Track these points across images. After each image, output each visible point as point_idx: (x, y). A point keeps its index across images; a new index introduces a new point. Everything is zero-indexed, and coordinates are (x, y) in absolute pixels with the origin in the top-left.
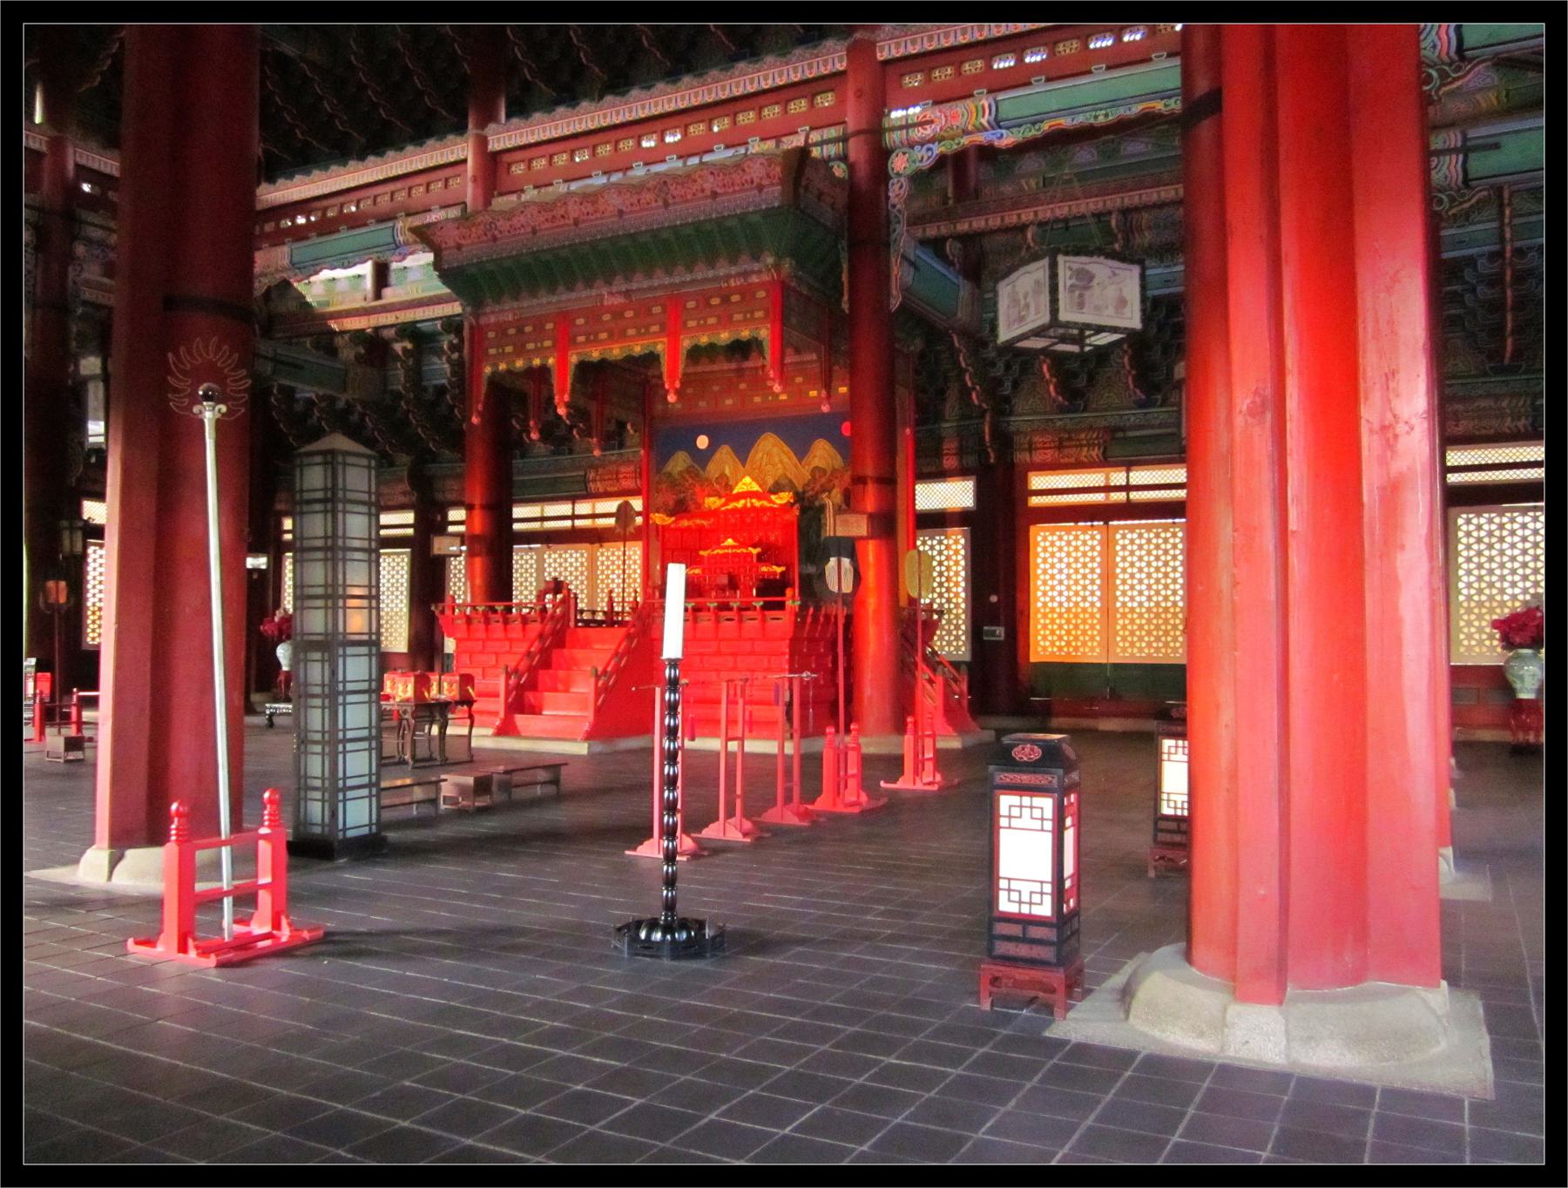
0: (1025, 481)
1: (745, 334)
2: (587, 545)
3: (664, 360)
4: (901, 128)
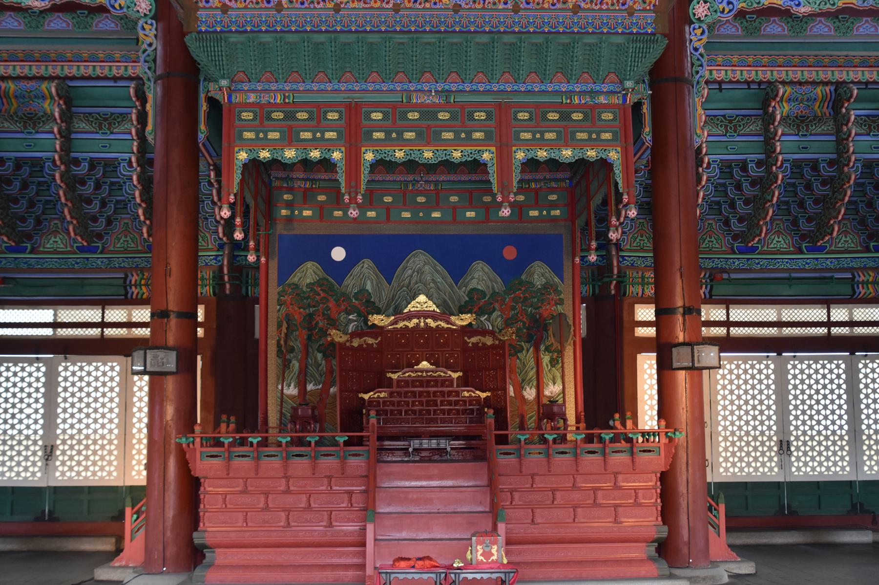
0: (632, 313)
1: (591, 154)
2: (122, 358)
3: (493, 170)
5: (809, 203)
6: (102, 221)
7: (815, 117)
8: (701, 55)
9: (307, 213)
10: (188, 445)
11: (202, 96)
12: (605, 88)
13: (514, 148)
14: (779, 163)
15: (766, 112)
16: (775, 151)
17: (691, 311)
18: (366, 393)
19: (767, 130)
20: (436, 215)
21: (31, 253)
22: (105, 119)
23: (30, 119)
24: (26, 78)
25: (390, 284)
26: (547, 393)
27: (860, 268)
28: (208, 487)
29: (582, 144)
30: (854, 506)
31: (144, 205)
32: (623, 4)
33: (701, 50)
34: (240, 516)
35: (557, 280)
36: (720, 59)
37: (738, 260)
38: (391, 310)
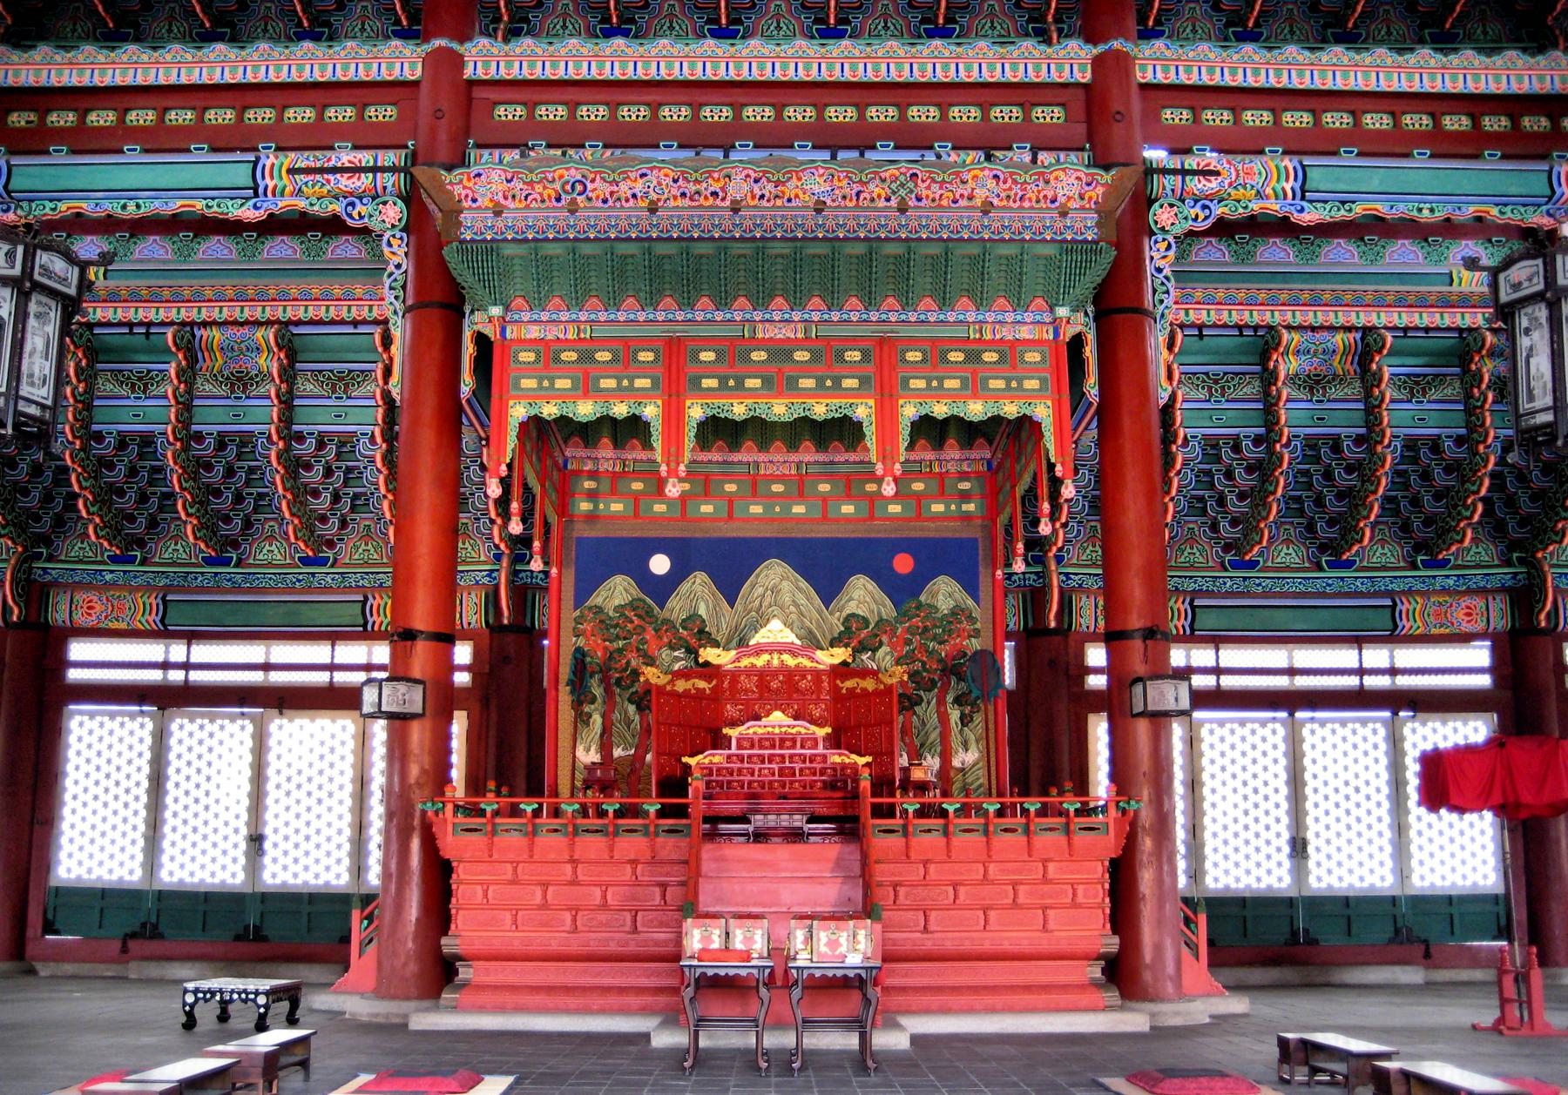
1: (1011, 410)
3: (870, 431)
4: (1174, 172)
5: (1329, 497)
6: (334, 522)
7: (1335, 376)
8: (1167, 278)
9: (616, 507)
10: (436, 813)
11: (467, 335)
12: (1029, 317)
13: (901, 402)
14: (1284, 440)
15: (1265, 369)
16: (1278, 422)
17: (1156, 635)
18: (692, 755)
19: (1267, 394)
20: (799, 509)
21: (237, 565)
22: (341, 379)
23: (240, 379)
24: (236, 323)
25: (732, 604)
26: (956, 763)
27: (1403, 592)
28: (461, 873)
29: (997, 396)
30: (1397, 931)
31: (390, 497)
32: (1053, 201)
33: (1167, 272)
34: (508, 916)
35: (970, 602)
36: (1199, 295)
37: (1232, 579)
38: (734, 643)
